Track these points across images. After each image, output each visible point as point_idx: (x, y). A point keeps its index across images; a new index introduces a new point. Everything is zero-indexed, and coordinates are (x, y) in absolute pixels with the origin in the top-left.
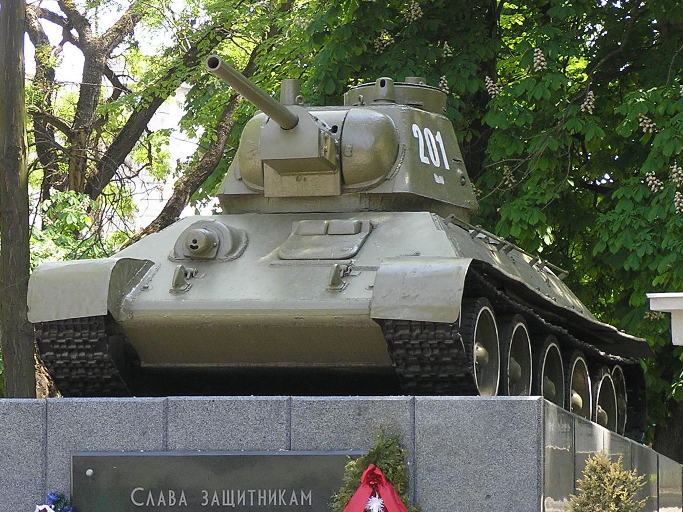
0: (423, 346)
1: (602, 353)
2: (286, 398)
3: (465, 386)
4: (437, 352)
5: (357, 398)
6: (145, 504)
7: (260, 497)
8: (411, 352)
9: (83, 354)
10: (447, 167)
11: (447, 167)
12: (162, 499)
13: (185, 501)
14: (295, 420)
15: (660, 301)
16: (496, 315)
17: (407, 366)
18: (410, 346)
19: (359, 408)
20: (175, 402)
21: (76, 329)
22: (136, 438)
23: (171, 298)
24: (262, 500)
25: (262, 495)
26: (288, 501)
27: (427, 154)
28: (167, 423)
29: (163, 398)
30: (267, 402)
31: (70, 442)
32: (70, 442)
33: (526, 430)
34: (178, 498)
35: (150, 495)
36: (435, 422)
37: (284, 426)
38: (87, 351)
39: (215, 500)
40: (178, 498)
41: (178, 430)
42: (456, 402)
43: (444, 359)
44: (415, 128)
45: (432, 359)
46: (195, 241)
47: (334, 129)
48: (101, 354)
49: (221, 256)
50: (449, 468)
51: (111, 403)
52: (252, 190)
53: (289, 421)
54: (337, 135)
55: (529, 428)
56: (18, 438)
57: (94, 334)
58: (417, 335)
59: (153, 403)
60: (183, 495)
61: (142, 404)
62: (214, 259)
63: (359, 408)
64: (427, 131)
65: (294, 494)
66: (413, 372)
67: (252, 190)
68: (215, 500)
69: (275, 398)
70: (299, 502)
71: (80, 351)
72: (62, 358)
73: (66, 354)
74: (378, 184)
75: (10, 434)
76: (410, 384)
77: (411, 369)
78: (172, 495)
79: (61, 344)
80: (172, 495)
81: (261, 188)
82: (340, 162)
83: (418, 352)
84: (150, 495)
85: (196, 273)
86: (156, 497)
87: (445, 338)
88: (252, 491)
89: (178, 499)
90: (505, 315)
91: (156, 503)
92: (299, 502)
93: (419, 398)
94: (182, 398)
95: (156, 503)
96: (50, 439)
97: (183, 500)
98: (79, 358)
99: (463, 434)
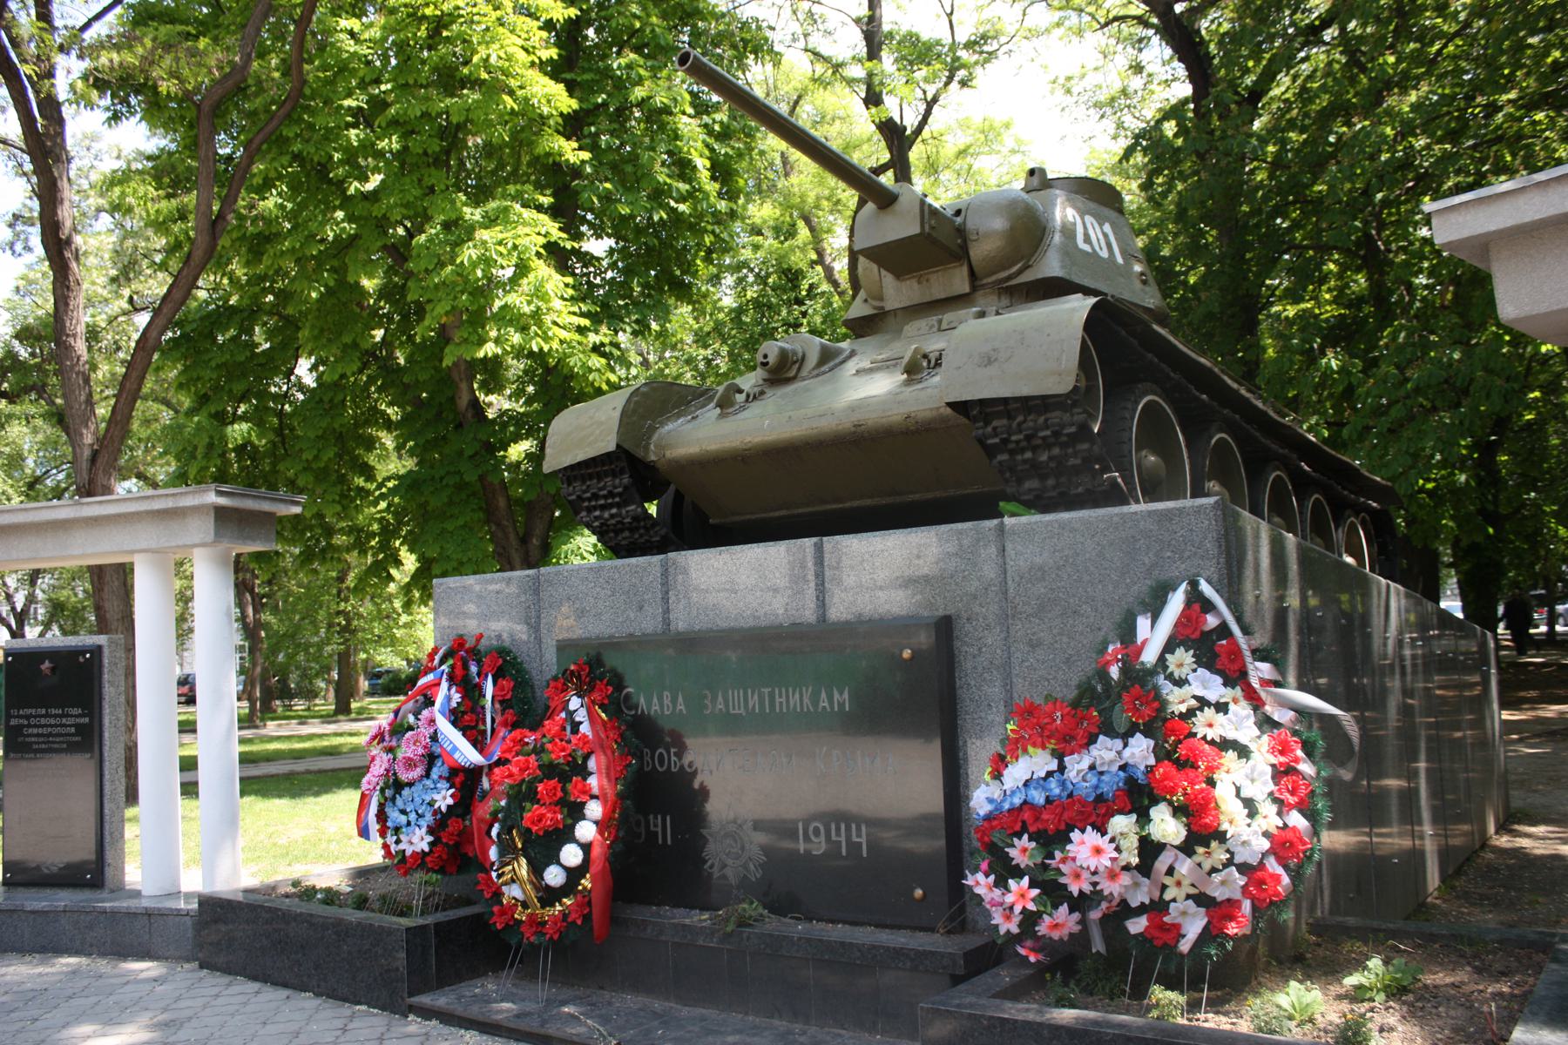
7: (778, 700)
8: (1019, 457)
9: (614, 511)
10: (1120, 260)
11: (1120, 260)
16: (1176, 411)
17: (1020, 481)
18: (1012, 446)
34: (674, 701)
36: (1038, 560)
38: (618, 505)
40: (674, 701)
42: (1070, 521)
43: (1072, 462)
45: (1052, 465)
46: (765, 356)
47: (958, 213)
49: (804, 373)
50: (1065, 639)
55: (1202, 557)
58: (1019, 424)
60: (680, 699)
62: (794, 379)
64: (1088, 219)
65: (823, 695)
71: (611, 506)
73: (597, 513)
74: (1020, 272)
77: (1028, 485)
83: (1028, 455)
87: (1063, 426)
88: (766, 690)
97: (681, 707)
98: (612, 516)
99: (1086, 578)
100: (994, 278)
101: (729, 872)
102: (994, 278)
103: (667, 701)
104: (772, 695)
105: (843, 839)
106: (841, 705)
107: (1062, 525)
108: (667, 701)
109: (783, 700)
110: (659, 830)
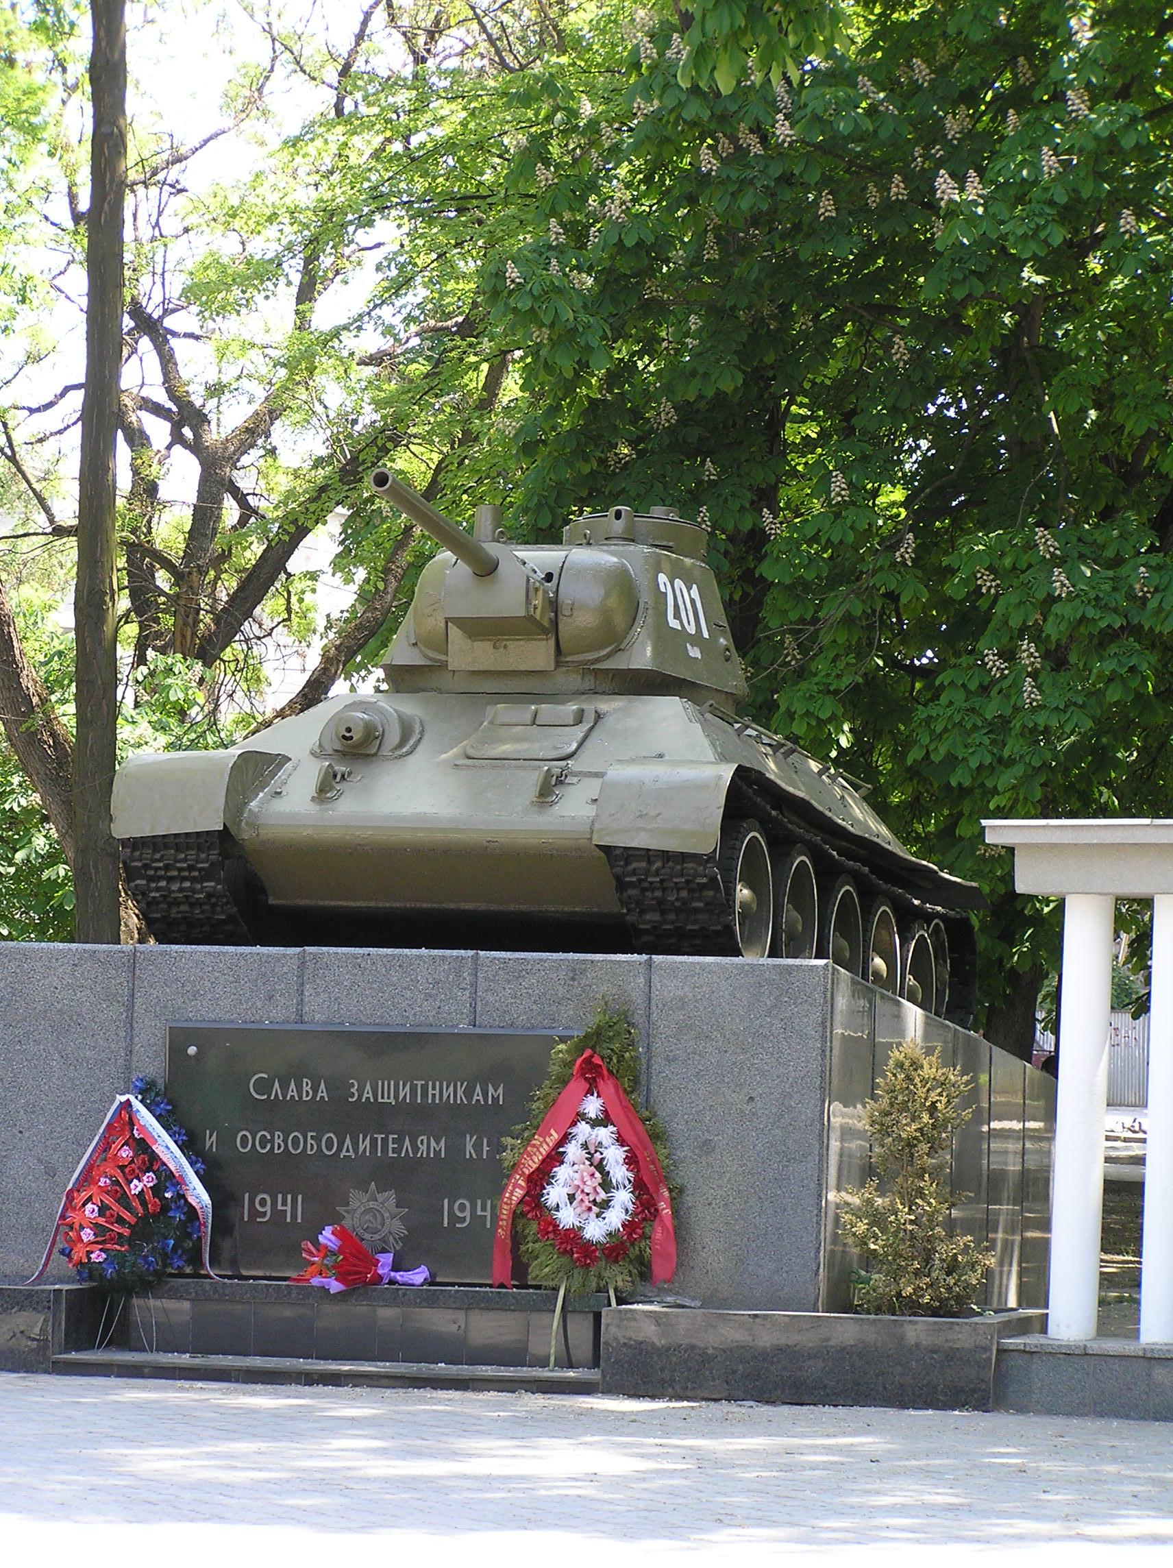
0: (665, 885)
1: (916, 902)
2: (471, 953)
3: (722, 943)
4: (684, 894)
5: (571, 955)
6: (269, 1097)
7: (431, 1092)
8: (648, 894)
9: (187, 884)
10: (706, 635)
11: (706, 635)
12: (292, 1091)
13: (325, 1094)
14: (482, 984)
15: (999, 831)
16: (768, 844)
17: (642, 912)
18: (646, 885)
19: (574, 970)
20: (315, 956)
21: (178, 849)
22: (259, 1004)
23: (313, 808)
24: (434, 1095)
25: (434, 1088)
26: (469, 1098)
27: (677, 616)
28: (302, 984)
29: (299, 949)
30: (443, 958)
31: (165, 1007)
32: (165, 1007)
33: (806, 1007)
34: (315, 1089)
35: (277, 1085)
36: (679, 993)
37: (467, 993)
38: (193, 880)
40: (315, 1089)
41: (318, 994)
42: (710, 964)
43: (695, 904)
44: (662, 578)
45: (677, 904)
46: (349, 730)
47: (549, 577)
48: (212, 884)
49: (385, 751)
51: (224, 954)
52: (430, 659)
53: (474, 985)
54: (551, 585)
55: (811, 1004)
56: (92, 999)
57: (203, 856)
58: (658, 870)
59: (284, 956)
60: (322, 1086)
61: (268, 956)
62: (375, 755)
63: (574, 970)
64: (678, 583)
66: (650, 922)
67: (430, 659)
68: (368, 1094)
69: (455, 952)
70: (486, 1100)
71: (184, 879)
72: (158, 889)
73: (163, 884)
74: (608, 656)
76: (645, 939)
77: (648, 917)
78: (307, 1086)
79: (157, 869)
80: (307, 1086)
81: (443, 658)
82: (555, 623)
83: (658, 894)
84: (277, 1085)
85: (349, 774)
86: (285, 1089)
87: (696, 875)
88: (419, 1083)
89: (315, 1091)
90: (781, 845)
91: (284, 1096)
92: (486, 1100)
93: (657, 958)
94: (325, 949)
95: (284, 1096)
96: (138, 1002)
97: (323, 1092)
99: (719, 1011)
100: (580, 657)
102: (580, 657)
107: (703, 967)
109: (437, 1092)
110: (289, 1208)
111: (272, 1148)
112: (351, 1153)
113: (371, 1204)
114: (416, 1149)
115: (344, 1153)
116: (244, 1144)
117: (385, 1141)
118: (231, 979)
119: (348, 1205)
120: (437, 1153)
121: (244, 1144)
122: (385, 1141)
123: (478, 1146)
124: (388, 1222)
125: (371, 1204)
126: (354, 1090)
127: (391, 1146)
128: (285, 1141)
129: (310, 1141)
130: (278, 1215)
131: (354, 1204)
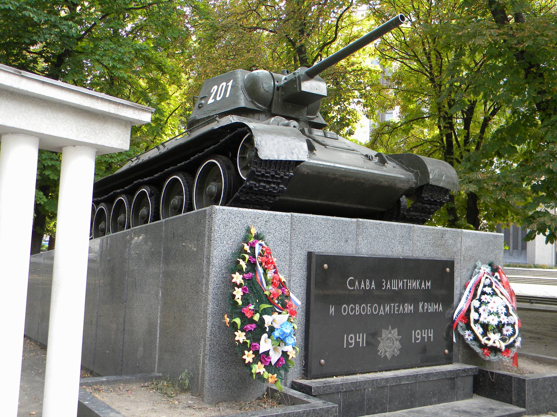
2: (411, 225)
22: (342, 244)
31: (305, 244)
34: (371, 284)
35: (357, 283)
36: (470, 244)
39: (388, 286)
40: (371, 284)
56: (274, 239)
61: (346, 222)
75: (270, 236)
84: (357, 283)
86: (360, 284)
88: (405, 280)
95: (360, 287)
101: (388, 354)
103: (368, 284)
104: (407, 282)
105: (426, 336)
106: (428, 287)
108: (368, 284)
110: (361, 340)
111: (355, 312)
112: (383, 313)
113: (390, 336)
114: (404, 309)
115: (380, 313)
116: (345, 311)
117: (394, 306)
118: (332, 232)
119: (381, 336)
120: (411, 311)
121: (345, 311)
122: (394, 306)
123: (423, 307)
124: (395, 342)
125: (390, 336)
126: (384, 284)
127: (396, 309)
128: (360, 309)
129: (369, 308)
130: (357, 343)
131: (384, 336)
